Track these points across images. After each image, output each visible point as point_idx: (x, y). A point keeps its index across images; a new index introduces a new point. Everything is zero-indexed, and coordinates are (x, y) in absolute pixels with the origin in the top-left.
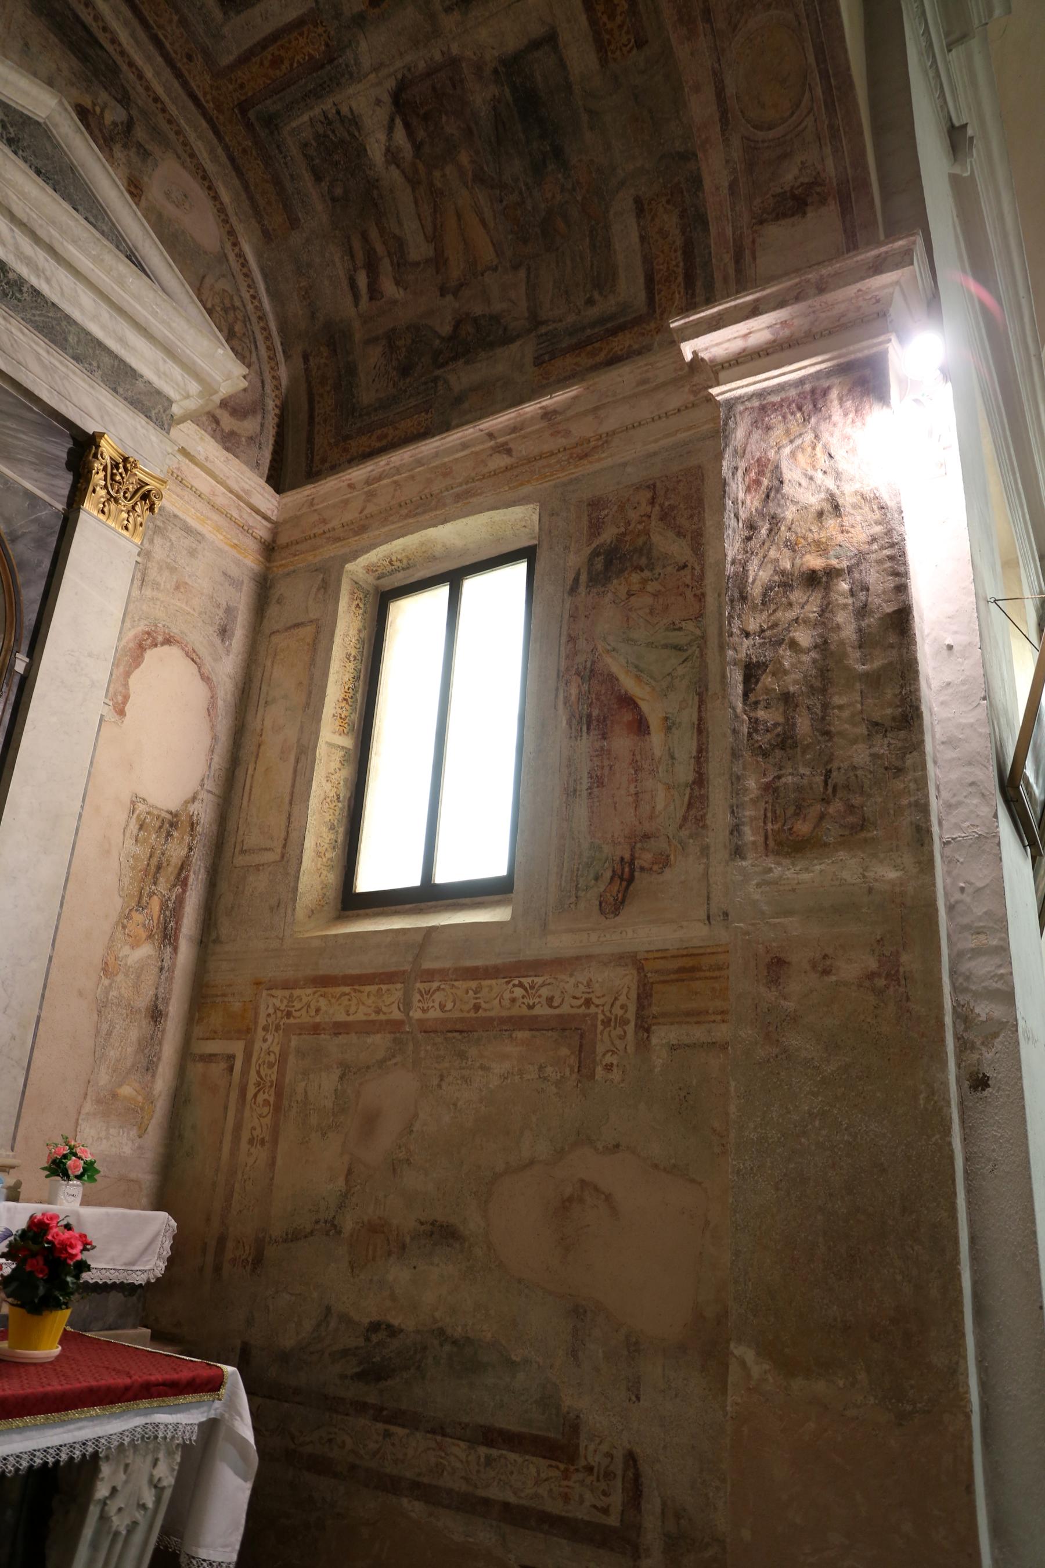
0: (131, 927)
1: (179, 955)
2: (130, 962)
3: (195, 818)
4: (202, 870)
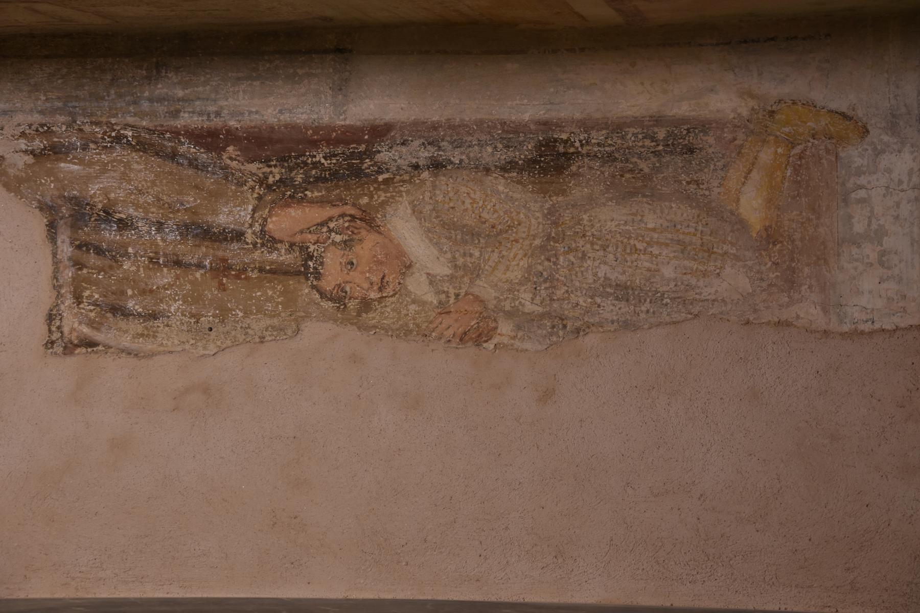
0: (360, 283)
1: (389, 117)
2: (442, 269)
3: (38, 144)
4: (161, 89)
